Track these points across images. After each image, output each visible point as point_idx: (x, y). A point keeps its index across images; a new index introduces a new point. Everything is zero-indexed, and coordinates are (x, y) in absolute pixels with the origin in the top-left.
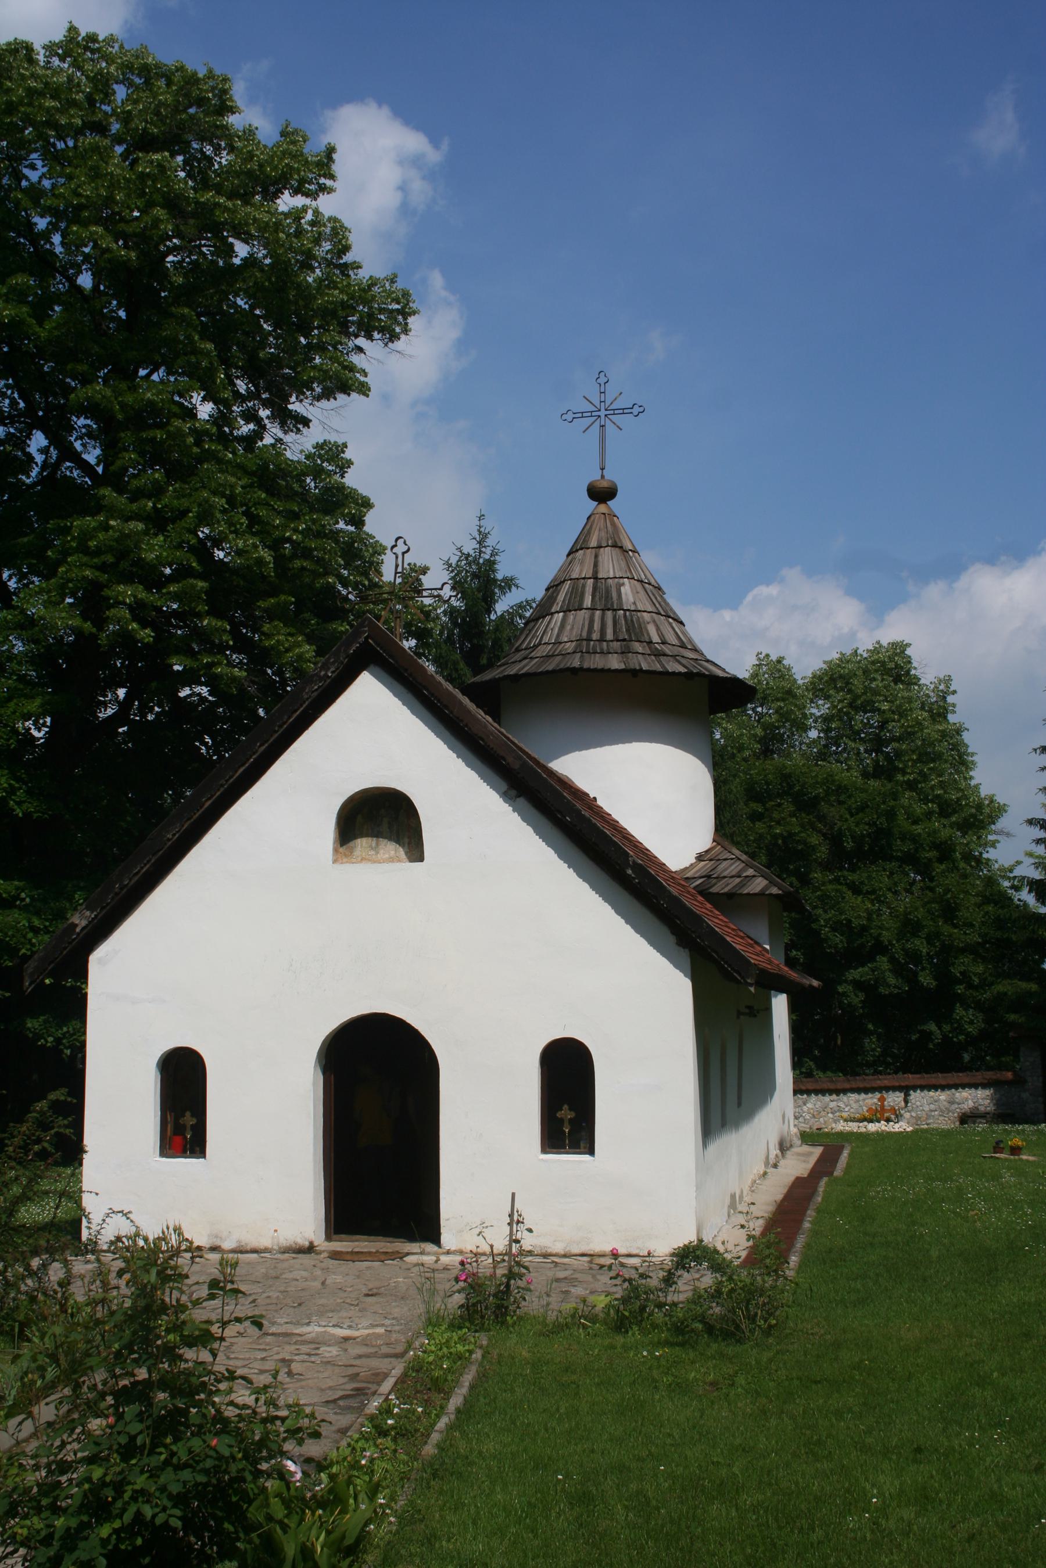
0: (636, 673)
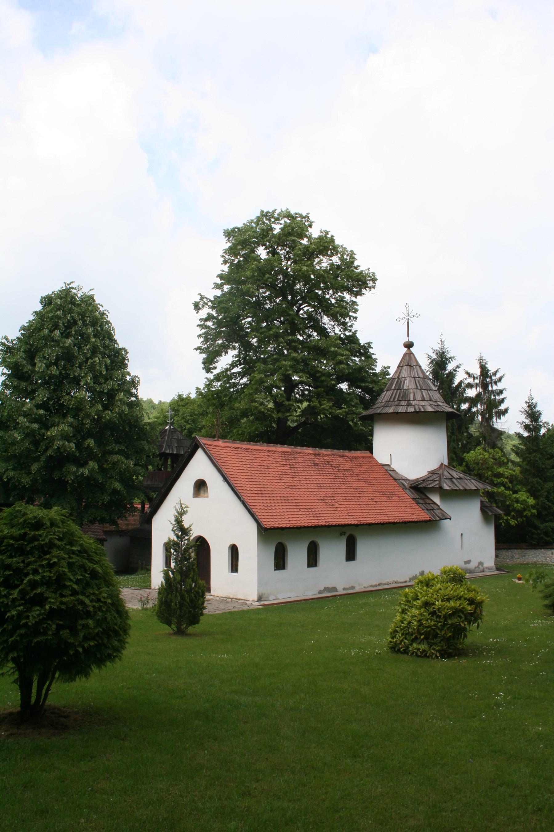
0: (397, 413)
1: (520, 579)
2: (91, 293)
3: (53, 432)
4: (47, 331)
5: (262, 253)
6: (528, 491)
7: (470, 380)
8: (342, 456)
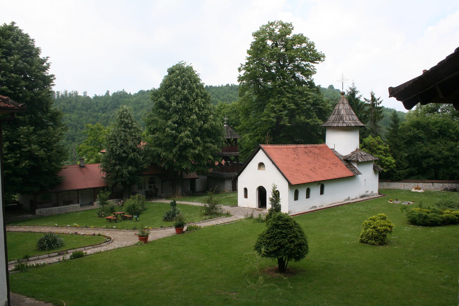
1: (391, 201)
2: (191, 65)
3: (183, 134)
4: (174, 87)
5: (269, 43)
6: (392, 156)
7: (367, 102)
8: (315, 147)
